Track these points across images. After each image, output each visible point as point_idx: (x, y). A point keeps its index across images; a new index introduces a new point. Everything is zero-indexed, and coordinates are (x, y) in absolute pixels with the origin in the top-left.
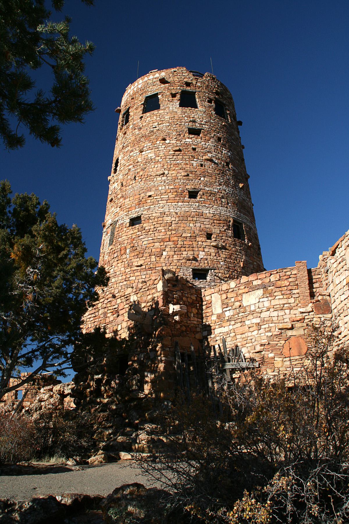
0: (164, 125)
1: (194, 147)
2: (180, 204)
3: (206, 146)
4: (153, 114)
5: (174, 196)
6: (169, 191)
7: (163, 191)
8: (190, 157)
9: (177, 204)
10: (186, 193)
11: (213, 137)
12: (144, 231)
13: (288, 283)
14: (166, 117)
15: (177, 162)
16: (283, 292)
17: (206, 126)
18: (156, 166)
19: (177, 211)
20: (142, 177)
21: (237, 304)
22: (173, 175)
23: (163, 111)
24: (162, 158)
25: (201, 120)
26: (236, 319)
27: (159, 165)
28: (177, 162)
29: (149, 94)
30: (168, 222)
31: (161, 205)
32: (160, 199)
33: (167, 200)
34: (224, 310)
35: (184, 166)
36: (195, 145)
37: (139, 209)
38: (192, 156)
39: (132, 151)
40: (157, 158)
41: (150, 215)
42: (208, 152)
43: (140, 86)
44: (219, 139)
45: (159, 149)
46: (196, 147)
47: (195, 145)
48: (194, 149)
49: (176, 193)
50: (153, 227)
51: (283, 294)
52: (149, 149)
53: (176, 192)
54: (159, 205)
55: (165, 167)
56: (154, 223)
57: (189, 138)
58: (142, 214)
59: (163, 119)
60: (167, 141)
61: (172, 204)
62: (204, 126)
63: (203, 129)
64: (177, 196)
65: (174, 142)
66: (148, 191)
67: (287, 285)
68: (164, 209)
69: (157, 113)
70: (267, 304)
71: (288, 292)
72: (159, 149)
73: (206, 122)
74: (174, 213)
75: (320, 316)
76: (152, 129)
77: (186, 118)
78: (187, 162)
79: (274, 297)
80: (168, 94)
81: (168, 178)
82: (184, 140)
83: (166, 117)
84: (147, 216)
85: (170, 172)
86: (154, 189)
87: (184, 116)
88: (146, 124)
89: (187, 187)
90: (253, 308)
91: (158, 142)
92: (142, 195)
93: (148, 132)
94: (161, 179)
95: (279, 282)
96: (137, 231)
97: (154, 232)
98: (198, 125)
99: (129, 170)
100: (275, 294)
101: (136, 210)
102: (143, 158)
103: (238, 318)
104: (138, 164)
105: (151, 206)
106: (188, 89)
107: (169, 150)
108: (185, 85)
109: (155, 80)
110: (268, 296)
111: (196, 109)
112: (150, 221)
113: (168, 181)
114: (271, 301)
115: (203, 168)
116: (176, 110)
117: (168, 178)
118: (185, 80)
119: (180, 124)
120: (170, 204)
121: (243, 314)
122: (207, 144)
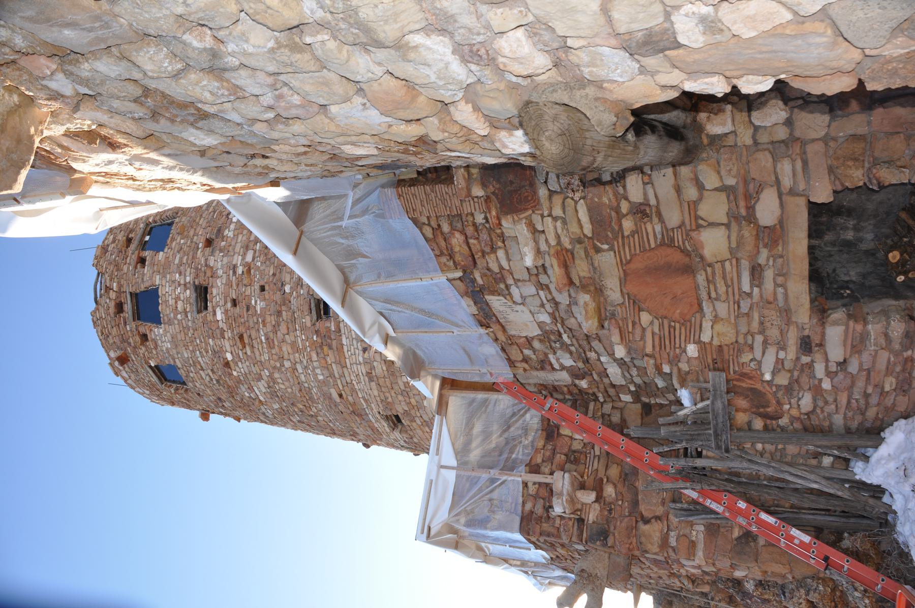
0: (200, 359)
1: (229, 305)
2: (344, 341)
3: (224, 275)
4: (187, 376)
5: (330, 352)
6: (323, 361)
7: (326, 372)
8: (250, 313)
9: (345, 348)
10: (321, 325)
11: (206, 260)
12: (413, 412)
13: (457, 235)
14: (186, 356)
15: (264, 341)
16: (487, 249)
17: (188, 274)
18: (280, 381)
19: (360, 348)
20: (307, 405)
21: (536, 344)
22: (290, 351)
23: (177, 360)
24: (262, 368)
25: (177, 282)
26: (581, 350)
27: (276, 375)
28: (264, 341)
29: (154, 379)
30: (384, 368)
31: (353, 378)
32: (343, 379)
33: (343, 367)
34: (557, 366)
35: (269, 328)
36: (226, 303)
37: (370, 417)
38: (248, 310)
39: (264, 414)
40: (265, 378)
41: (378, 399)
42: (235, 273)
43: (148, 392)
44: (209, 243)
45: (247, 372)
46: (229, 299)
47: (226, 303)
48: (235, 303)
49: (325, 348)
50: (400, 398)
51: (494, 250)
52: (251, 389)
53: (321, 346)
54: (354, 382)
55: (278, 365)
56: (393, 395)
57: (215, 314)
58: (379, 413)
59: (191, 362)
60: (229, 357)
61: (347, 356)
62: (188, 279)
63: (194, 282)
64: (330, 347)
65: (227, 345)
66: (330, 398)
67: (462, 238)
68: (361, 374)
69: (183, 371)
70: (530, 289)
71: (484, 236)
72: (247, 372)
73: (180, 274)
74: (366, 355)
75: (542, 192)
76: (215, 382)
77: (179, 316)
78: (260, 320)
79: (506, 274)
80: (143, 349)
81: (298, 360)
82: (220, 324)
83: (186, 356)
84: (381, 405)
85: (286, 356)
86: (325, 389)
87: (176, 322)
88: (208, 390)
89: (309, 324)
90: (545, 318)
91: (235, 373)
92: (341, 408)
93: (221, 387)
94: (303, 376)
95: (458, 258)
96: (414, 424)
97: (411, 395)
98: (188, 292)
99: (299, 421)
100: (496, 269)
101: (374, 421)
102: (271, 400)
103: (577, 345)
104: (284, 408)
105: (360, 396)
106: (128, 307)
107: (245, 355)
108: (122, 315)
109: (127, 369)
110: (502, 286)
111: (160, 294)
112: (390, 400)
113: (305, 362)
114: (516, 281)
115: (267, 288)
116: (168, 335)
117: (298, 360)
118: (112, 315)
119: (191, 331)
120: (347, 361)
121: (565, 337)
122: (220, 272)
